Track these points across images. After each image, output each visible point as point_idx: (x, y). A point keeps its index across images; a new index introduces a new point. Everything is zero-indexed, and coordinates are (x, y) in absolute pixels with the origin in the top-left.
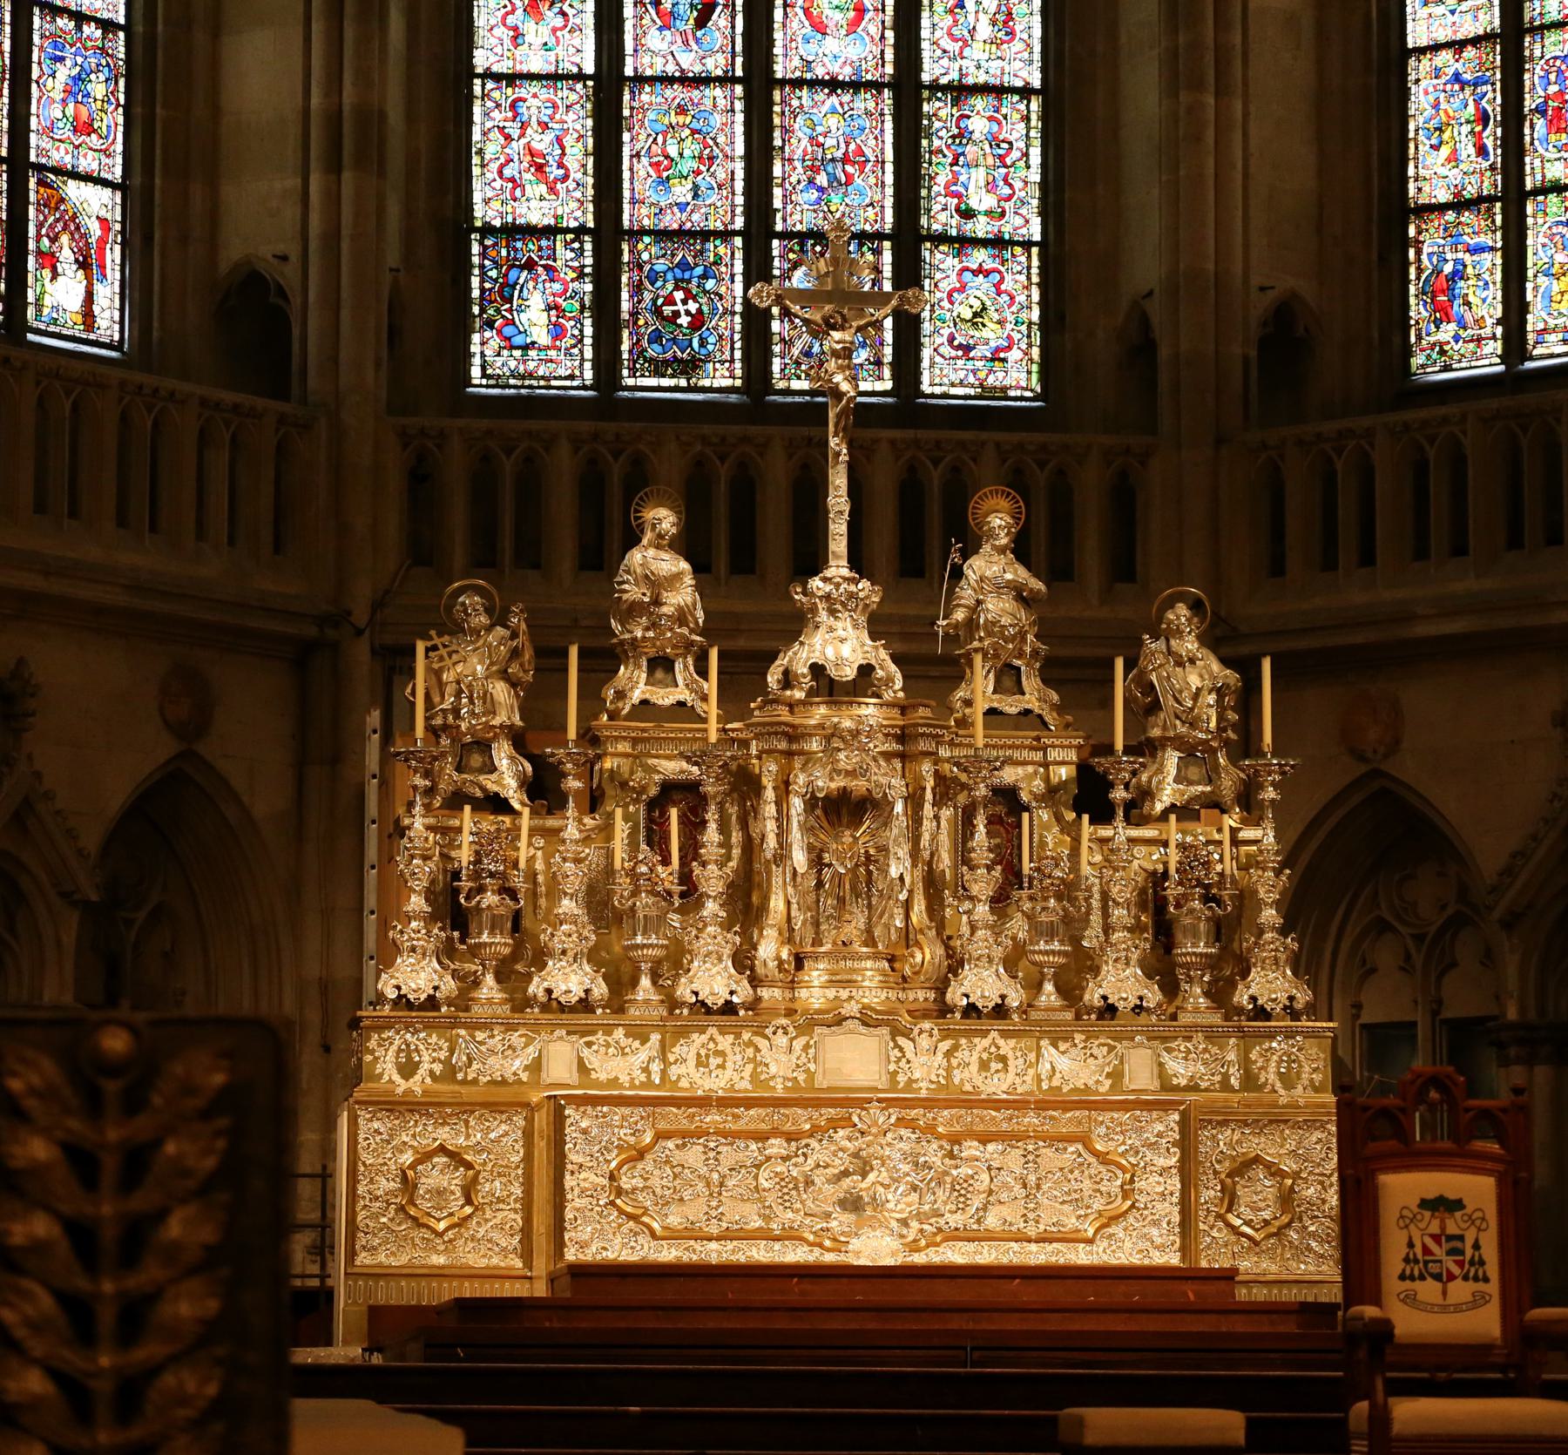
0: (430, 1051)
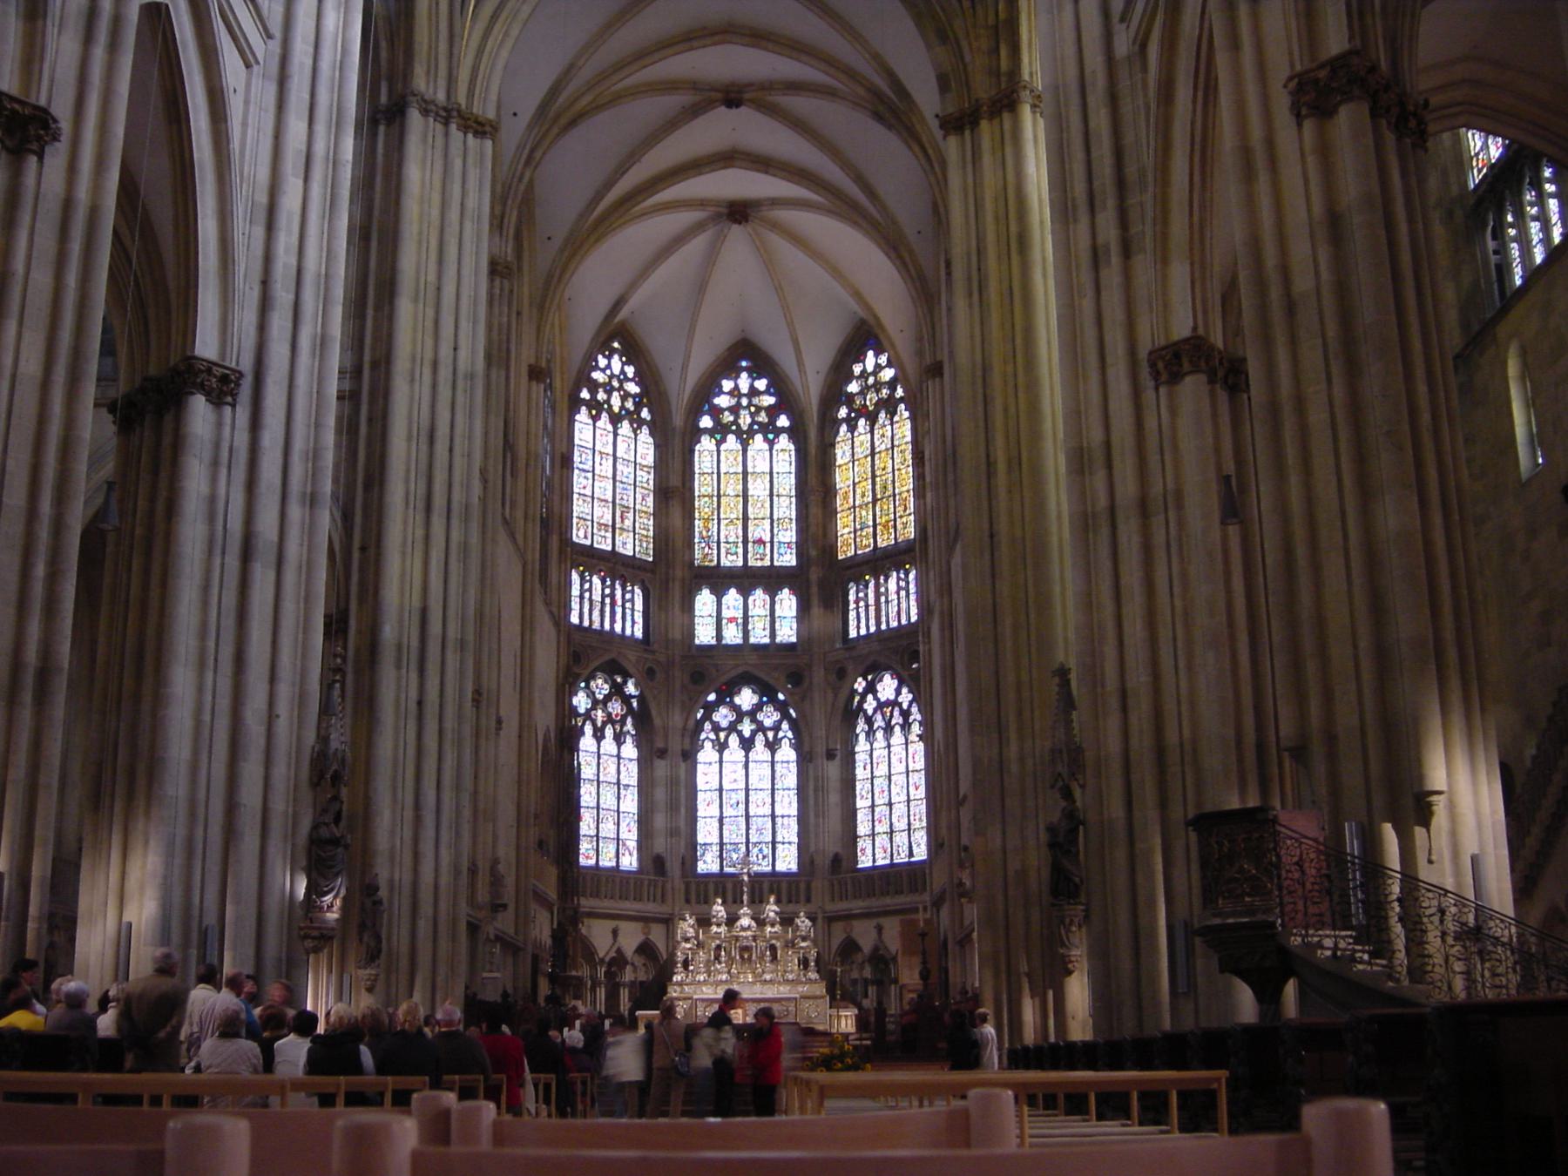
0: (678, 989)
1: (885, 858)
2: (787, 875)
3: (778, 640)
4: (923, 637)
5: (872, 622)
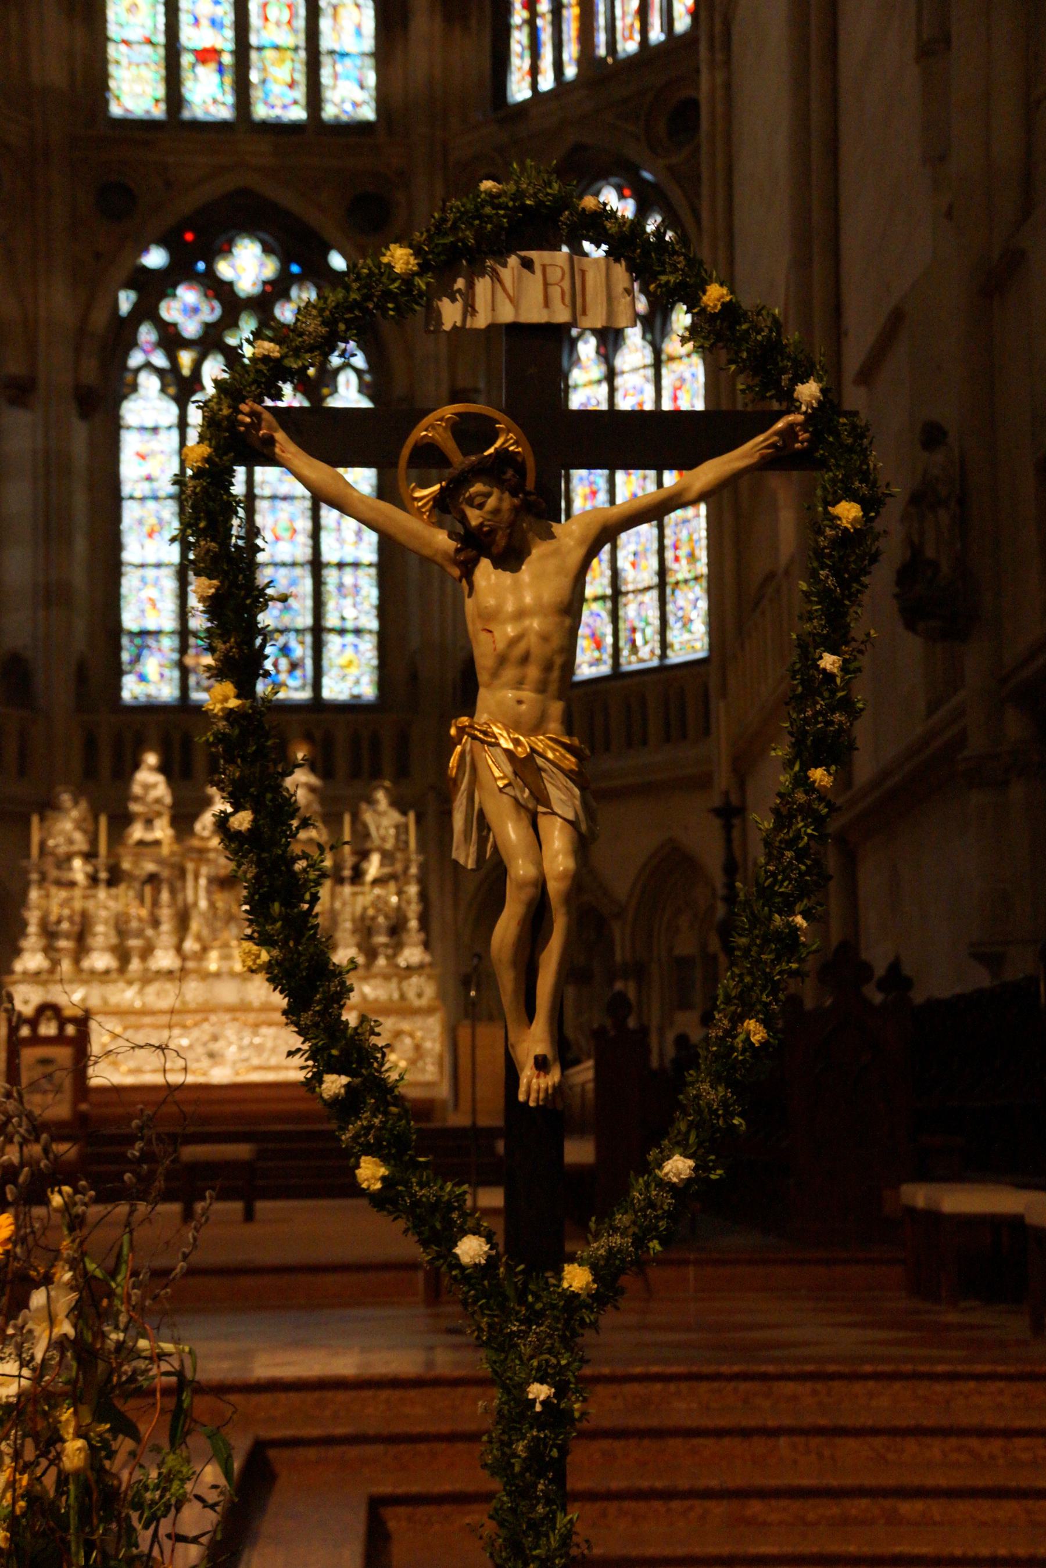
1: (597, 662)
2: (352, 708)
3: (329, 112)
4: (711, 48)
5: (571, 51)
